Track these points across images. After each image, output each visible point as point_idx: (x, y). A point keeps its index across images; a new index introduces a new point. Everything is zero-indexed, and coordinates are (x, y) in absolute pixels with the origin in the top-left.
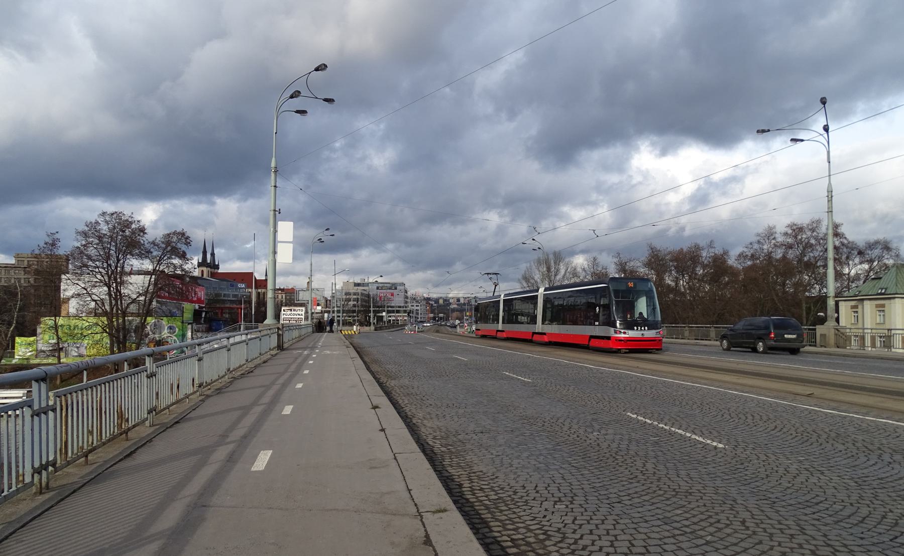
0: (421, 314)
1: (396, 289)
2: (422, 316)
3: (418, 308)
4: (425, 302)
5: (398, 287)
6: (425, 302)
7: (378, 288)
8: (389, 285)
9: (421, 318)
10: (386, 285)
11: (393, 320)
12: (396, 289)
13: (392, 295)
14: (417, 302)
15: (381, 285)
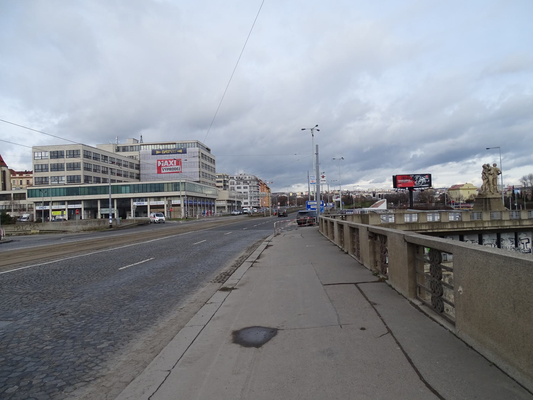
0: (251, 198)
1: (184, 152)
2: (253, 200)
3: (247, 190)
4: (256, 183)
5: (188, 150)
6: (256, 183)
7: (154, 153)
8: (172, 147)
9: (251, 203)
10: (169, 147)
11: (152, 207)
12: (184, 152)
13: (179, 162)
14: (245, 182)
15: (161, 147)
